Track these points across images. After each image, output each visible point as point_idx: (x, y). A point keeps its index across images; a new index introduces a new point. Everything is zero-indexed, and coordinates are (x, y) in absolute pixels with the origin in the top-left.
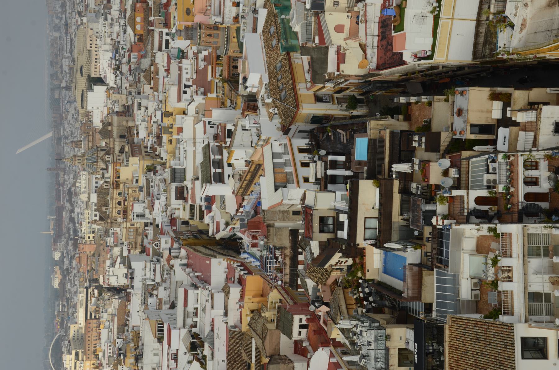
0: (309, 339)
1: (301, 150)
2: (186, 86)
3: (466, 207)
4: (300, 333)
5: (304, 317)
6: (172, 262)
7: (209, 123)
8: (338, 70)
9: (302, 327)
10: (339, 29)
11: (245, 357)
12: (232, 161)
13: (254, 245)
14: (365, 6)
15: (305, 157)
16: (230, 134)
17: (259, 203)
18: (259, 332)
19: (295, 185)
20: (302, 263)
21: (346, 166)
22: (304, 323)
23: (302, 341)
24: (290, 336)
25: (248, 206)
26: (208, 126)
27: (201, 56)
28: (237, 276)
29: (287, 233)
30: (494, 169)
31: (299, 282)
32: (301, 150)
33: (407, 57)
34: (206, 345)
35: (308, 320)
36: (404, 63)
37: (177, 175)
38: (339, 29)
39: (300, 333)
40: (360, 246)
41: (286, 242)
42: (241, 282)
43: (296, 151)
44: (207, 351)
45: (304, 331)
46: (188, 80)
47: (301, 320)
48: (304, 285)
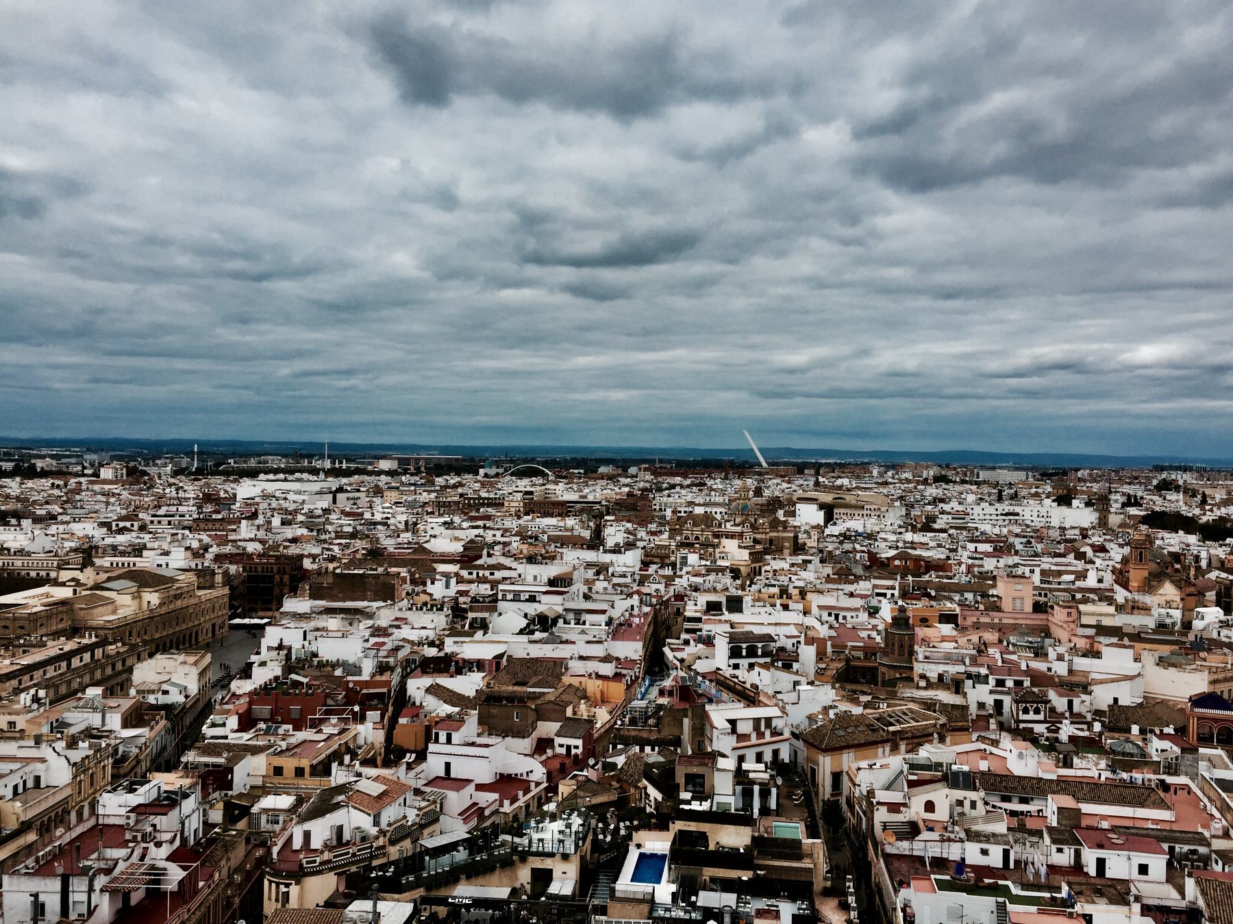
0: (555, 756)
1: (776, 753)
2: (837, 617)
4: (561, 746)
5: (579, 751)
6: (636, 597)
7: (799, 642)
8: (878, 803)
10: (930, 807)
11: (534, 680)
12: (757, 669)
13: (662, 693)
14: (961, 841)
15: (768, 757)
16: (787, 667)
17: (711, 701)
18: (563, 697)
19: (735, 745)
20: (642, 750)
21: (765, 811)
22: (574, 751)
23: (553, 748)
24: (558, 734)
25: (709, 687)
26: (795, 641)
27: (874, 634)
28: (624, 672)
29: (677, 733)
31: (619, 747)
32: (776, 753)
33: (904, 893)
34: (545, 635)
35: (576, 755)
36: (896, 891)
37: (735, 605)
38: (930, 807)
39: (561, 746)
40: (671, 825)
41: (667, 733)
42: (618, 676)
43: (775, 746)
44: (538, 635)
45: (563, 751)
46: (845, 618)
47: (576, 747)
48: (618, 753)
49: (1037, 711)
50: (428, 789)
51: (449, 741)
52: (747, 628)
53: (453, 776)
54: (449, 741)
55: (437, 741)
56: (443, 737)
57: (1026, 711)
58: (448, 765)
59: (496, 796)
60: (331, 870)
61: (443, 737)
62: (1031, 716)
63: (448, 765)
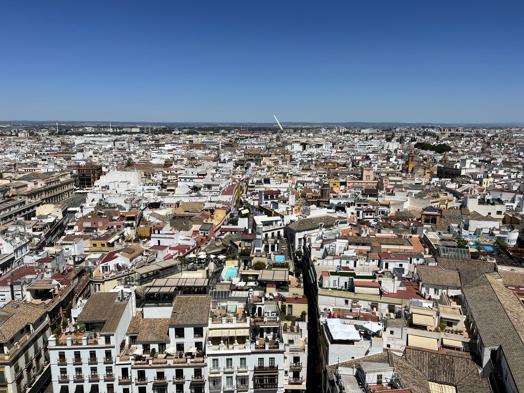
2: (303, 184)
3: (257, 303)
9: (204, 233)
16: (285, 202)
22: (206, 235)
27: (316, 190)
30: (273, 315)
34: (196, 194)
37: (267, 181)
44: (193, 194)
45: (203, 235)
49: (371, 215)
50: (151, 250)
51: (159, 233)
52: (271, 189)
53: (161, 245)
54: (159, 233)
55: (154, 233)
56: (156, 232)
57: (367, 215)
58: (159, 241)
59: (177, 251)
60: (115, 279)
61: (156, 232)
62: (369, 216)
63: (159, 241)
